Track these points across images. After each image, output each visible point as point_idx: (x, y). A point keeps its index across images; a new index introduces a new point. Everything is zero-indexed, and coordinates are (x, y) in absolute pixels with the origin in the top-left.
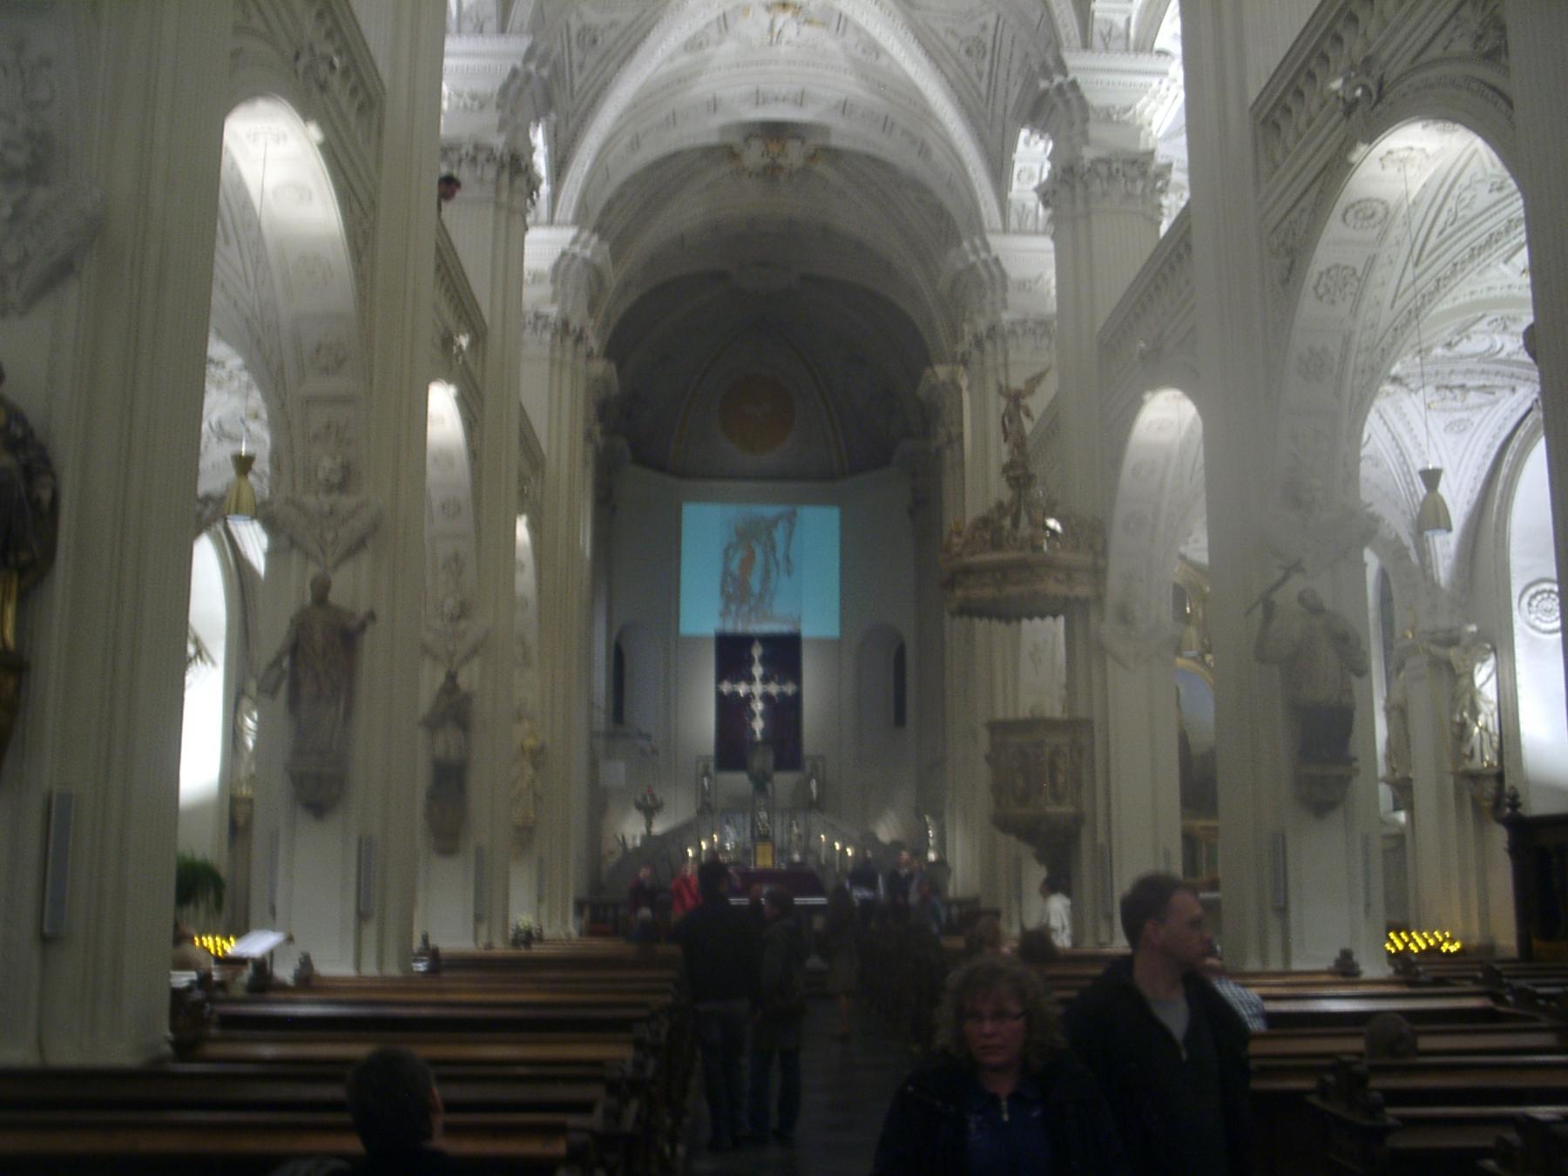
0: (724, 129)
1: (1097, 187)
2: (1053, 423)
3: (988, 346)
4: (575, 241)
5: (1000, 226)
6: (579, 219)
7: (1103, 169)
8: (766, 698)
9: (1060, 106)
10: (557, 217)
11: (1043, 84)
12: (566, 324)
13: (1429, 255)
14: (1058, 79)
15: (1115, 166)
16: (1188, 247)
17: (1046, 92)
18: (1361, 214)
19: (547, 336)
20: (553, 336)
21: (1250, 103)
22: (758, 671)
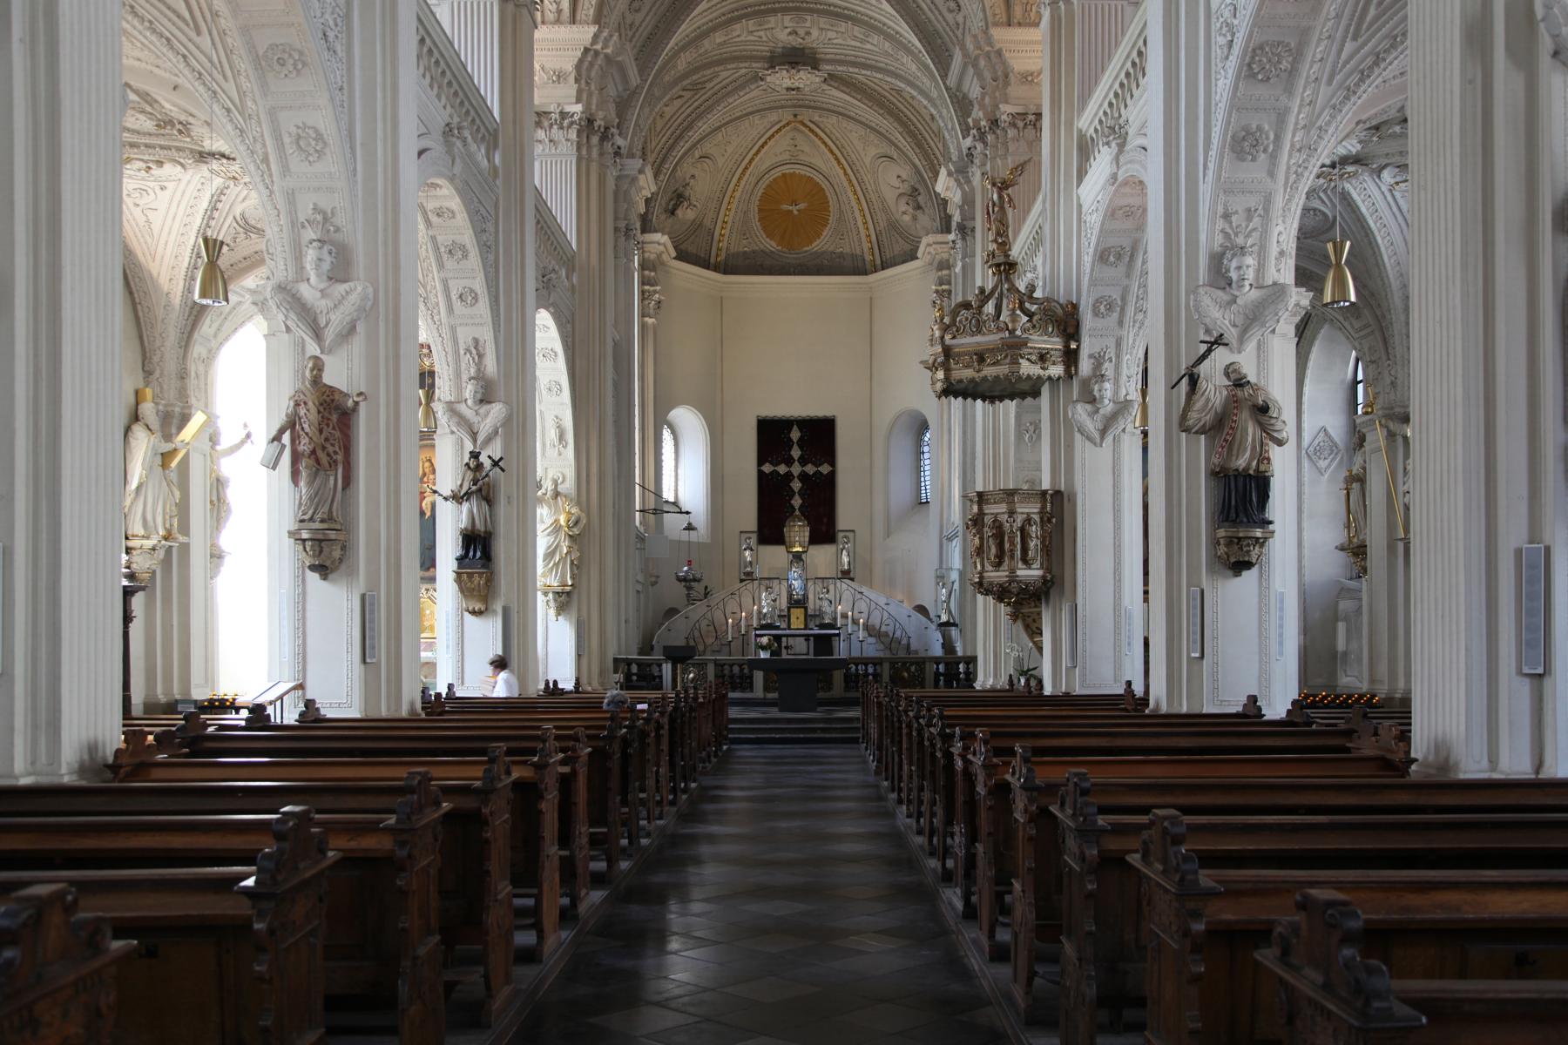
4: (596, 37)
5: (1004, 19)
6: (598, 19)
10: (578, 18)
12: (590, 121)
19: (573, 135)
20: (579, 132)
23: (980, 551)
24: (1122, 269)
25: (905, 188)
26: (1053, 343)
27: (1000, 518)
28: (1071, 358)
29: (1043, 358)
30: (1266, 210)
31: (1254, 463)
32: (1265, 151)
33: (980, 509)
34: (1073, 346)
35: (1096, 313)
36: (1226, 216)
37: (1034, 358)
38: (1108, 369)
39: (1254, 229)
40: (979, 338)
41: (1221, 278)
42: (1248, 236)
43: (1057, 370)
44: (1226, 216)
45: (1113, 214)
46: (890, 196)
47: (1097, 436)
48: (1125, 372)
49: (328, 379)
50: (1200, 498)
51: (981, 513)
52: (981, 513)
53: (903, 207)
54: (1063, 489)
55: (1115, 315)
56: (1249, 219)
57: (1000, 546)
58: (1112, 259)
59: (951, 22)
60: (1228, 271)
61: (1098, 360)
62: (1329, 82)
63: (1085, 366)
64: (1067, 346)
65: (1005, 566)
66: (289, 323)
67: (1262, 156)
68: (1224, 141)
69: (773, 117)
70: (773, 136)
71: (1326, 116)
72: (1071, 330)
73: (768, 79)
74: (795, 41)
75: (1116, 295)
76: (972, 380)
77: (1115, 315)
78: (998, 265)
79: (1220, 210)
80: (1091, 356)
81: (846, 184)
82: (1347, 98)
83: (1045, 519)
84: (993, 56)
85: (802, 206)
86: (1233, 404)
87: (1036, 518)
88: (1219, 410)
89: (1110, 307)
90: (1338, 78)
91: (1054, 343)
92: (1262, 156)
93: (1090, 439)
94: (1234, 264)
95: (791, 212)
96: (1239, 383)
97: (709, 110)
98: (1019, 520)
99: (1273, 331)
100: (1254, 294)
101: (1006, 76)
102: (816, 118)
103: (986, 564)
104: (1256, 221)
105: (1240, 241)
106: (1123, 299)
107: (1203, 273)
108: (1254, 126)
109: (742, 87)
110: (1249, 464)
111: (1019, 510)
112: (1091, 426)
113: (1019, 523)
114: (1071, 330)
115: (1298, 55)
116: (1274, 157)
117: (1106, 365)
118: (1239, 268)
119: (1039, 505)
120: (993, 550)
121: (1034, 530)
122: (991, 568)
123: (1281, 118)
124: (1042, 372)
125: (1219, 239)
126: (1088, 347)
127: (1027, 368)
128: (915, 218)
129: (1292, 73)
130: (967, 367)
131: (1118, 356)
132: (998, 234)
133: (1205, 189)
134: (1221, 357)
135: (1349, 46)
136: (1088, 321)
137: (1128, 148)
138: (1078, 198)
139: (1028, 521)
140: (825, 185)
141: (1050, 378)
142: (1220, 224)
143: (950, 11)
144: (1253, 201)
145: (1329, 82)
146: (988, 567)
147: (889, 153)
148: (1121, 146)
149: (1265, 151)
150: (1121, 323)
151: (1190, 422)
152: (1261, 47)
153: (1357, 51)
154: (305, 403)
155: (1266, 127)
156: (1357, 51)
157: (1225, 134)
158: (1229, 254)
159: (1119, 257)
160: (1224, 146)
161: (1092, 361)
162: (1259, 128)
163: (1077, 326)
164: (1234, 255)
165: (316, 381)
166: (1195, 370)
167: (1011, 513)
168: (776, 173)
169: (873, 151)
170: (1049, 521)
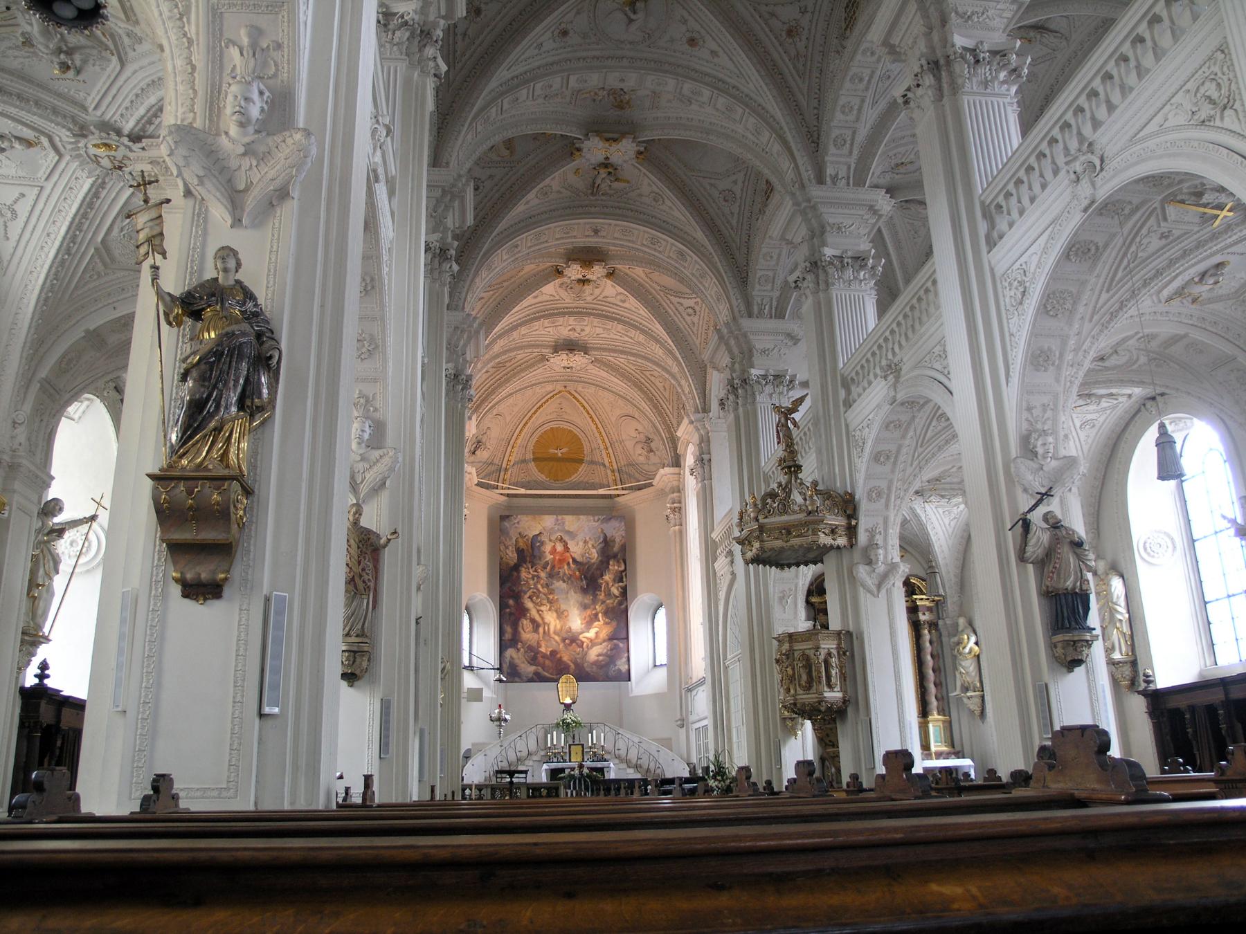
13: (1118, 283)
15: (846, 260)
23: (792, 679)
24: (888, 467)
25: (642, 437)
26: (838, 521)
27: (807, 652)
28: (852, 531)
29: (833, 531)
30: (1056, 405)
32: (1053, 364)
33: (791, 647)
34: (854, 522)
35: (870, 499)
36: (1029, 409)
37: (827, 531)
38: (879, 539)
39: (1048, 419)
40: (785, 518)
41: (1029, 451)
42: (1044, 423)
43: (842, 541)
44: (1029, 409)
45: (887, 427)
46: (629, 444)
47: (874, 589)
48: (890, 542)
49: (364, 522)
50: (1036, 613)
51: (791, 650)
52: (791, 650)
53: (639, 451)
54: (851, 629)
55: (883, 501)
56: (1044, 411)
57: (810, 674)
58: (882, 459)
59: (689, 322)
60: (1035, 447)
61: (872, 533)
62: (1091, 321)
63: (862, 538)
64: (849, 524)
65: (814, 689)
67: (1051, 368)
68: (1026, 357)
69: (549, 387)
70: (547, 401)
71: (1088, 343)
73: (552, 360)
74: (573, 335)
75: (883, 485)
76: (782, 550)
77: (883, 501)
78: (789, 467)
79: (1024, 404)
80: (867, 530)
81: (597, 435)
82: (1101, 331)
83: (841, 653)
85: (565, 450)
86: (1056, 541)
87: (834, 652)
88: (1047, 546)
89: (879, 495)
90: (1096, 318)
92: (1051, 368)
94: (1040, 443)
97: (507, 381)
99: (1070, 490)
100: (1054, 463)
101: (751, 351)
102: (580, 389)
103: (798, 689)
104: (1049, 414)
105: (1039, 426)
106: (889, 488)
107: (1014, 449)
108: (1046, 348)
109: (532, 365)
111: (822, 646)
112: (870, 582)
113: (822, 657)
115: (1076, 300)
116: (1059, 368)
117: (878, 537)
118: (1044, 444)
119: (836, 642)
120: (804, 677)
121: (834, 661)
122: (802, 692)
123: (1064, 340)
125: (1025, 426)
126: (864, 523)
127: (824, 539)
128: (648, 458)
129: (1072, 312)
130: (777, 539)
131: (886, 530)
132: (787, 446)
133: (1011, 394)
134: (1042, 510)
135: (1104, 296)
136: (864, 507)
137: (902, 380)
138: (846, 420)
139: (829, 654)
140: (581, 435)
142: (1025, 415)
143: (690, 315)
144: (1046, 399)
145: (1091, 321)
146: (800, 691)
147: (631, 414)
148: (897, 378)
149: (1053, 364)
150: (887, 506)
151: (1028, 555)
152: (1054, 293)
153: (1108, 300)
155: (1054, 348)
156: (1108, 300)
157: (1027, 353)
158: (1034, 435)
159: (888, 457)
160: (1026, 361)
161: (868, 534)
162: (1050, 349)
163: (855, 509)
164: (1040, 436)
165: (356, 523)
166: (1028, 517)
167: (817, 648)
168: (547, 427)
169: (618, 412)
170: (844, 654)
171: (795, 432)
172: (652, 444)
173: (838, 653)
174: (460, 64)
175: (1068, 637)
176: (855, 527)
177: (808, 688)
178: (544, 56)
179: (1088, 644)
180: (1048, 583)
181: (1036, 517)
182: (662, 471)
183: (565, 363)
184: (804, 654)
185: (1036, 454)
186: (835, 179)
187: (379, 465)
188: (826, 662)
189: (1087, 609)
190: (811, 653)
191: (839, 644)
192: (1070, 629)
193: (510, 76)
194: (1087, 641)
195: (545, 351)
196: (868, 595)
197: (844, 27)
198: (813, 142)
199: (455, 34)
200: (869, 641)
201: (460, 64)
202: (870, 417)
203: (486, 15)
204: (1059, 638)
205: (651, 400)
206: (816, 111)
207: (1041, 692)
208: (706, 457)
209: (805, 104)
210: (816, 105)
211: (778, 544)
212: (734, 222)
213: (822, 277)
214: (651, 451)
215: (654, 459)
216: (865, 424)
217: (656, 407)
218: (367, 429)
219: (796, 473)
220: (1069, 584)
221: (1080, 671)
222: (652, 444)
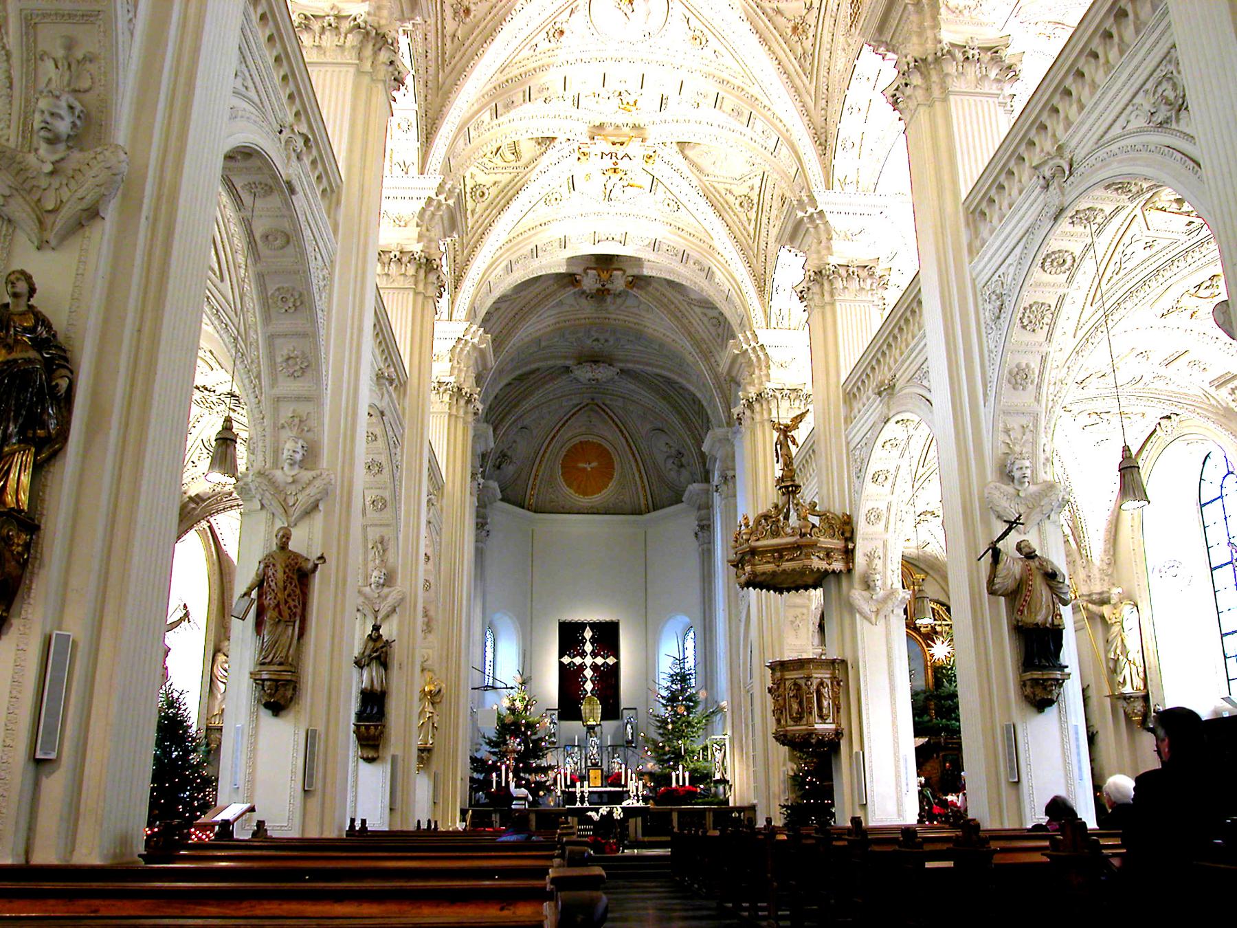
0: (572, 260)
1: (839, 284)
2: (811, 448)
3: (757, 406)
7: (843, 272)
8: (595, 667)
9: (812, 230)
11: (800, 214)
12: (460, 389)
14: (811, 210)
15: (851, 270)
16: (920, 302)
17: (802, 220)
18: (1055, 264)
19: (446, 398)
21: (964, 196)
22: (588, 648)
25: (673, 451)
27: (799, 681)
28: (849, 554)
30: (1036, 426)
31: (1050, 619)
34: (850, 546)
37: (822, 555)
38: (878, 564)
39: (1026, 441)
46: (660, 458)
48: (890, 566)
55: (882, 523)
60: (1011, 471)
61: (870, 557)
63: (860, 560)
64: (846, 547)
66: (264, 502)
72: (848, 535)
76: (774, 574)
77: (882, 523)
78: (787, 487)
84: (758, 349)
88: (1018, 577)
91: (837, 543)
93: (866, 618)
95: (585, 469)
96: (1030, 556)
98: (815, 683)
100: (1032, 488)
104: (1028, 436)
108: (1024, 366)
110: (1046, 619)
112: (867, 608)
114: (848, 535)
117: (876, 561)
124: (828, 567)
127: (817, 563)
128: (679, 473)
130: (769, 562)
132: (785, 464)
134: (1014, 538)
139: (821, 684)
141: (834, 571)
142: (1002, 437)
154: (274, 565)
155: (1033, 366)
161: (866, 558)
167: (809, 678)
169: (648, 426)
171: (794, 450)
172: (683, 460)
173: (832, 683)
174: (450, 67)
175: (1037, 675)
176: (853, 550)
177: (798, 720)
178: (539, 57)
179: (1059, 683)
180: (1019, 618)
181: (1008, 546)
182: (690, 487)
183: (590, 375)
184: (795, 684)
185: (1012, 479)
186: (843, 183)
187: (312, 486)
188: (819, 692)
189: (1059, 646)
190: (802, 682)
191: (833, 674)
192: (1042, 668)
193: (504, 79)
194: (1057, 680)
195: (568, 363)
196: (866, 622)
197: (850, 23)
198: (820, 144)
199: (444, 36)
200: (865, 667)
201: (450, 67)
202: (868, 436)
203: (475, 16)
204: (1028, 675)
205: (678, 413)
206: (823, 112)
207: (1008, 732)
208: (730, 473)
209: (813, 104)
210: (824, 106)
211: (770, 567)
212: (751, 229)
213: (826, 286)
214: (682, 466)
215: (685, 474)
216: (863, 443)
217: (684, 421)
218: (299, 450)
219: (794, 492)
220: (1039, 619)
221: (1052, 712)
222: (683, 460)
